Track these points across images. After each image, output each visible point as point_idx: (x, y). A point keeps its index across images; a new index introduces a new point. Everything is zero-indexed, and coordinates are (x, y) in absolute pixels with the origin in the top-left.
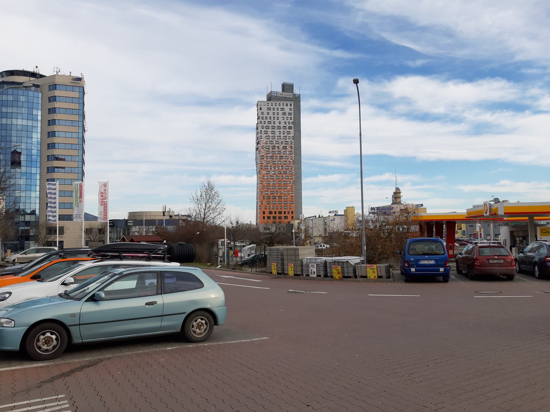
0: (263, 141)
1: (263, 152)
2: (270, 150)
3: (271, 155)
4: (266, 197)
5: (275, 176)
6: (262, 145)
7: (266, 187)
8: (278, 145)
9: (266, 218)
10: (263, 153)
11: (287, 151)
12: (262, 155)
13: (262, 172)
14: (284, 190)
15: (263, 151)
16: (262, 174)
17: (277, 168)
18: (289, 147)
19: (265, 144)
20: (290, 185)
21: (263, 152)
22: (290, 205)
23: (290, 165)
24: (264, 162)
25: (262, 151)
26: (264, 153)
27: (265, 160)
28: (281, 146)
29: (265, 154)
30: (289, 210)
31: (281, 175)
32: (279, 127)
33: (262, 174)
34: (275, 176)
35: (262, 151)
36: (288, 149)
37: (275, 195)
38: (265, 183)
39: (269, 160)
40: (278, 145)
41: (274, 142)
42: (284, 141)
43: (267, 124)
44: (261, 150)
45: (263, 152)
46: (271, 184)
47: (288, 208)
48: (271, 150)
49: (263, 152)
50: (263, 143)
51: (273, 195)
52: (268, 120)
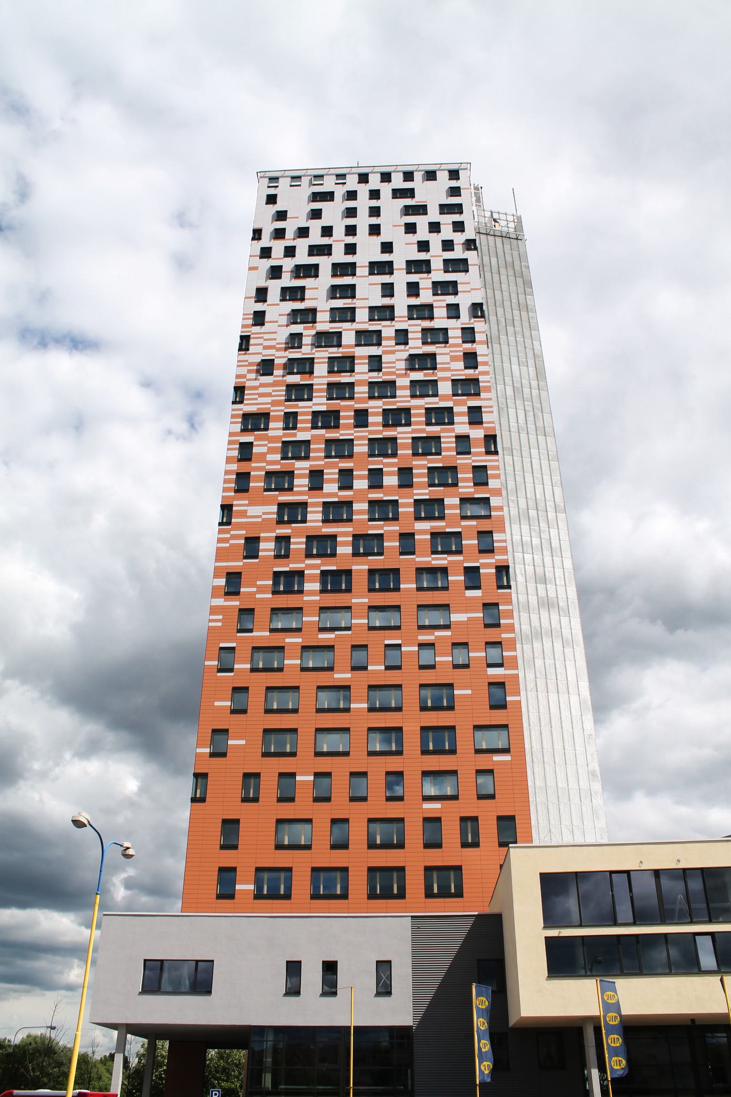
0: (266, 336)
1: (268, 390)
2: (315, 381)
3: (320, 403)
4: (256, 700)
5: (345, 534)
6: (258, 359)
7: (262, 615)
8: (374, 351)
9: (245, 887)
10: (261, 400)
11: (444, 379)
12: (253, 409)
13: (243, 514)
14: (425, 637)
15: (263, 385)
16: (240, 526)
17: (361, 484)
18: (454, 359)
19: (278, 350)
20: (470, 593)
21: (268, 390)
22: (484, 762)
23: (463, 461)
24: (264, 450)
25: (256, 388)
26: (269, 400)
27: (272, 439)
28: (393, 352)
29: (274, 403)
30: (469, 806)
31: (392, 528)
32: (380, 268)
33: (240, 526)
34: (345, 534)
35: (256, 388)
36: (448, 369)
37: (342, 676)
38: (261, 589)
39: (301, 436)
40: (374, 351)
41: (349, 338)
42: (415, 328)
43: (302, 257)
44: (248, 384)
45: (262, 390)
46: (312, 593)
47: (468, 793)
48: (325, 381)
49: (262, 390)
50: (273, 343)
51: (324, 678)
52: (316, 238)
